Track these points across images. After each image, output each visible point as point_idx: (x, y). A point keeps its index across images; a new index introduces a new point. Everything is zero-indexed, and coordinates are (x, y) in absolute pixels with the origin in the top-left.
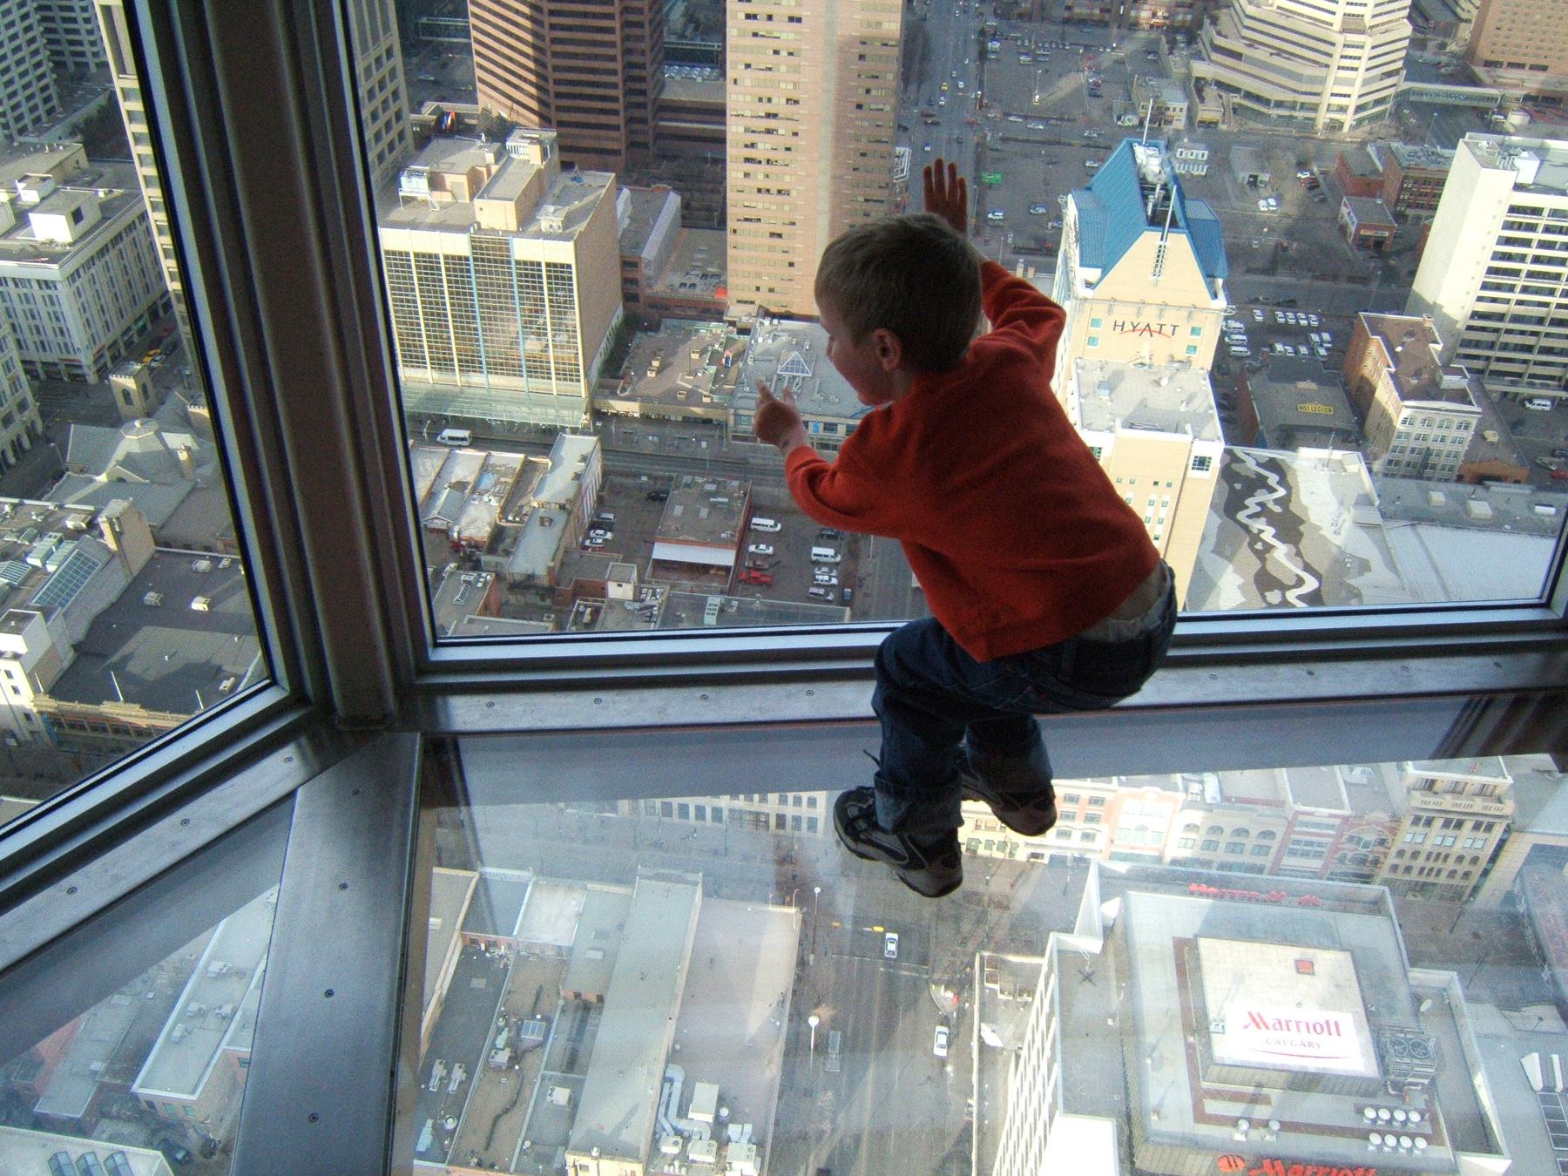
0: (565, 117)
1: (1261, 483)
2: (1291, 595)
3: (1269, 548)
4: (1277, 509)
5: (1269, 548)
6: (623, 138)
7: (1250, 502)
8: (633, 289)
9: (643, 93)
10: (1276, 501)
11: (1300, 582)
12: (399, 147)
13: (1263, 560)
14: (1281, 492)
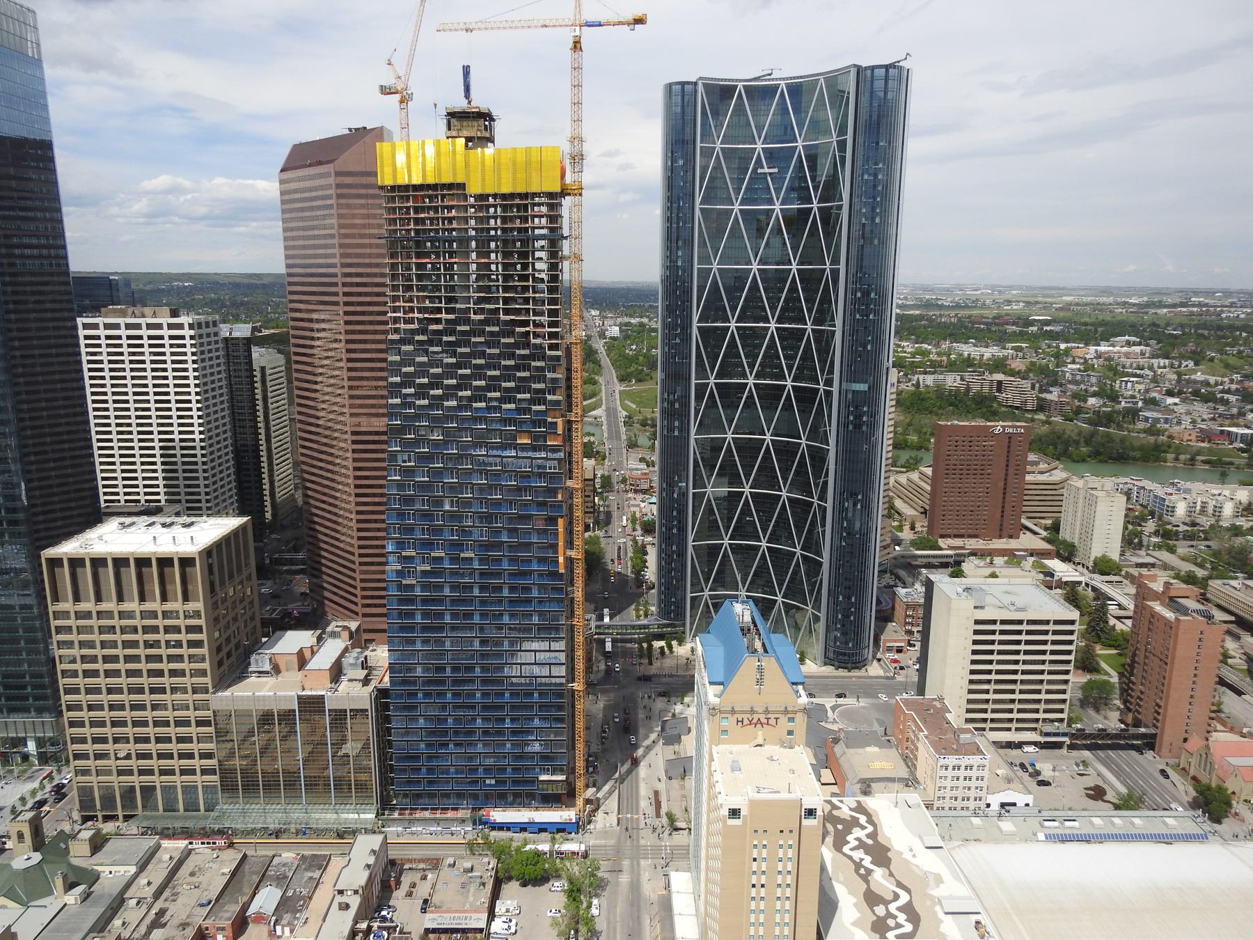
0: (368, 610)
1: (855, 823)
2: (892, 908)
3: (869, 872)
4: (870, 842)
5: (869, 872)
7: (849, 838)
10: (868, 836)
13: (867, 882)
14: (870, 829)
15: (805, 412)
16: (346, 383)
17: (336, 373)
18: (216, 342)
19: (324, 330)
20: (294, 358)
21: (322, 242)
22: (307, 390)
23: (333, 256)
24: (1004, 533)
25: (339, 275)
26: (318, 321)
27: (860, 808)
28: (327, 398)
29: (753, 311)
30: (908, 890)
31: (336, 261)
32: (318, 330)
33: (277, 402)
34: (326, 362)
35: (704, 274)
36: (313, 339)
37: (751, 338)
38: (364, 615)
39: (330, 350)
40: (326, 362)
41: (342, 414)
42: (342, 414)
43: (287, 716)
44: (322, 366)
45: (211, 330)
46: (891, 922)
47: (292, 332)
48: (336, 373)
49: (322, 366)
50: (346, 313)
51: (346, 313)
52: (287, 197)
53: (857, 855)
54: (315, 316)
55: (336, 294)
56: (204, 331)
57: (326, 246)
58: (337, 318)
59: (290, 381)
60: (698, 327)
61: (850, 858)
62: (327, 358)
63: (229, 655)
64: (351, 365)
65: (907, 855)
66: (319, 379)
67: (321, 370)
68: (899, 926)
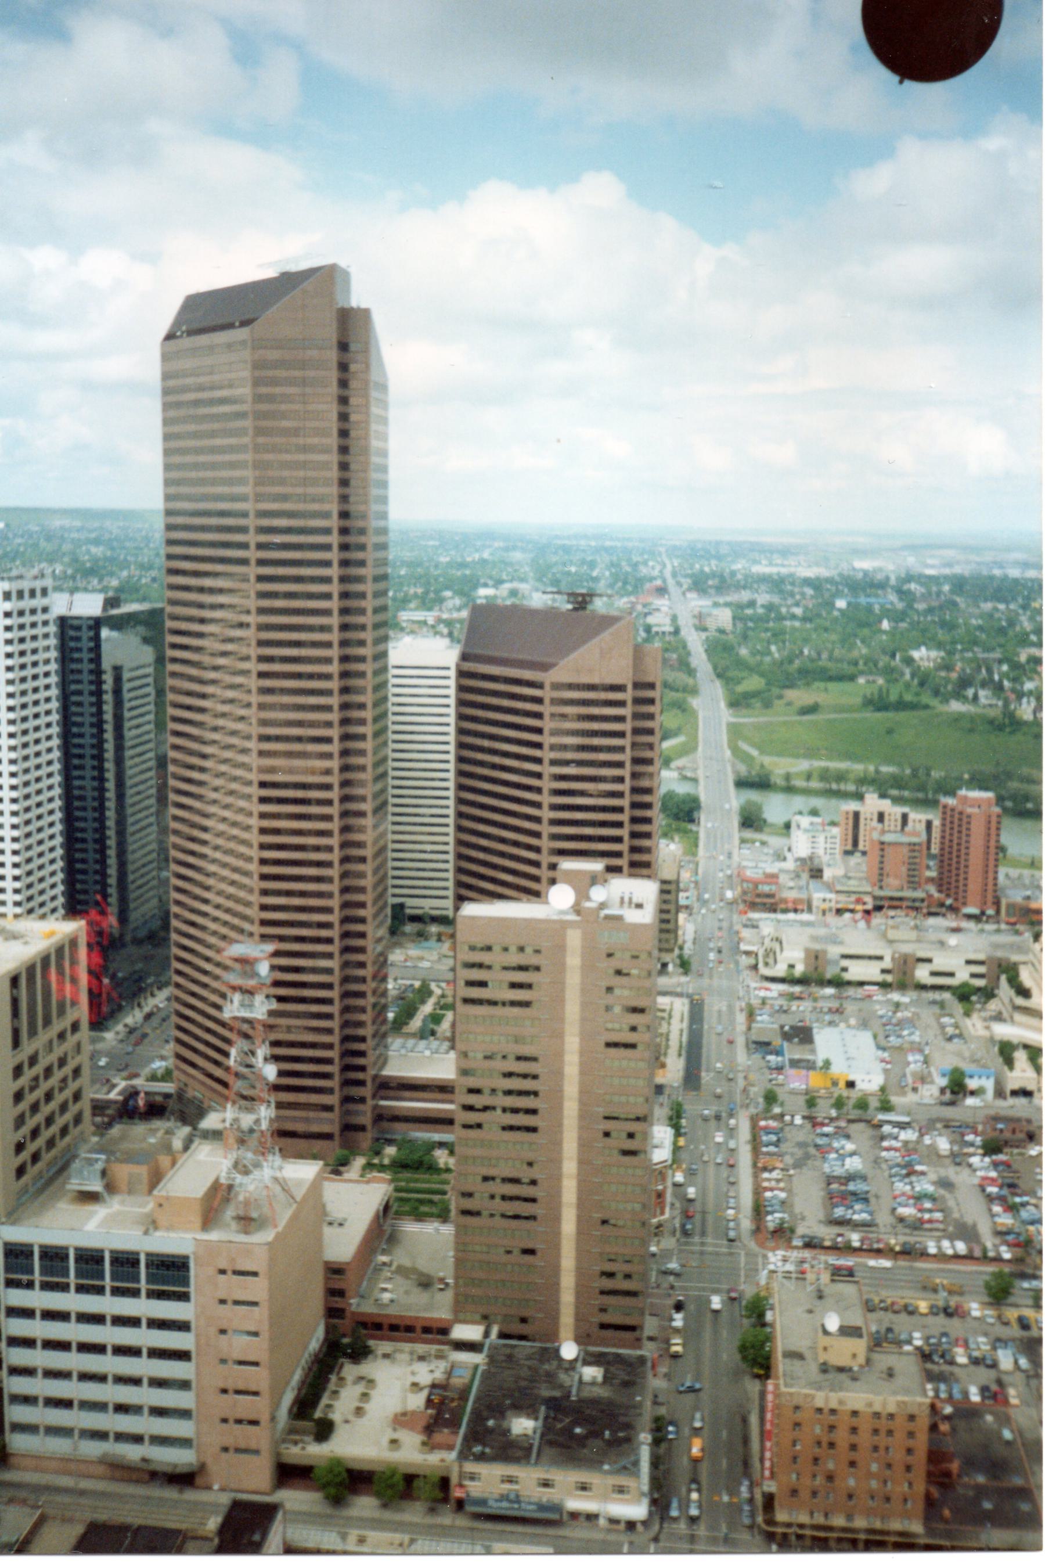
6: (337, 1120)
8: (338, 1302)
12: (74, 1132)
16: (254, 699)
17: (239, 680)
18: (45, 623)
19: (221, 606)
20: (170, 653)
21: (227, 458)
22: (189, 708)
23: (242, 481)
25: (252, 514)
26: (211, 591)
28: (221, 722)
31: (247, 490)
32: (213, 607)
33: (138, 726)
34: (221, 661)
36: (202, 621)
39: (231, 640)
40: (221, 661)
41: (245, 751)
42: (245, 751)
44: (216, 668)
45: (38, 602)
47: (169, 609)
48: (239, 680)
49: (216, 668)
50: (261, 579)
51: (261, 579)
52: (171, 383)
54: (207, 582)
55: (245, 546)
56: (27, 604)
57: (232, 465)
58: (244, 586)
59: (160, 693)
62: (224, 654)
63: (35, 1157)
64: (265, 667)
67: (212, 675)
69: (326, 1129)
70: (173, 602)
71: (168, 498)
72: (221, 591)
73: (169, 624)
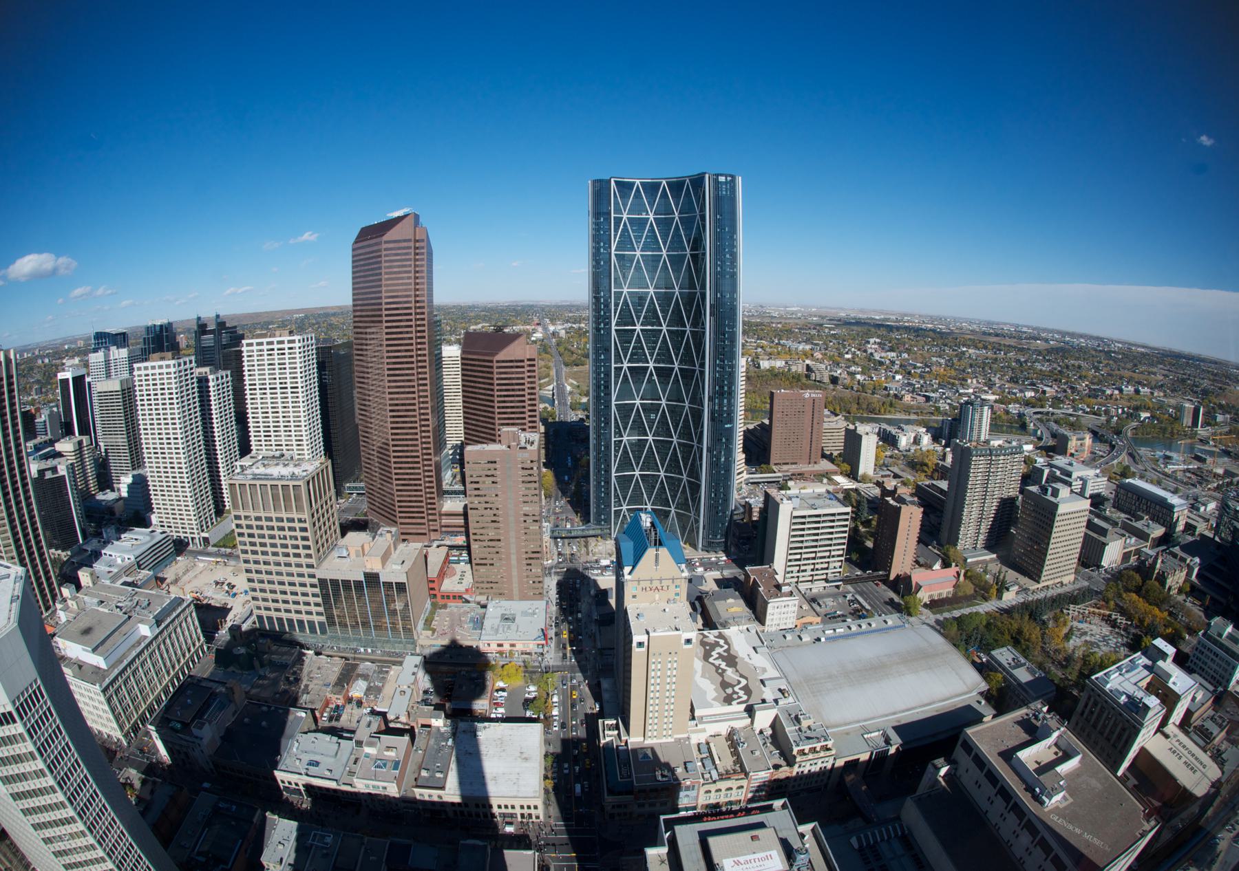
1: (717, 644)
2: (736, 689)
3: (724, 671)
4: (725, 654)
5: (724, 671)
7: (713, 653)
9: (434, 509)
11: (739, 682)
13: (723, 677)
14: (726, 647)
15: (687, 386)
24: (812, 461)
26: (370, 333)
27: (721, 636)
29: (652, 318)
30: (746, 679)
32: (370, 339)
35: (618, 295)
36: (366, 345)
37: (652, 336)
38: (401, 524)
43: (358, 584)
46: (735, 696)
53: (717, 663)
54: (368, 330)
60: (616, 330)
61: (713, 664)
65: (747, 659)
66: (370, 370)
67: (370, 365)
68: (739, 697)
69: (423, 531)
70: (356, 339)
71: (354, 300)
72: (373, 333)
73: (355, 347)
